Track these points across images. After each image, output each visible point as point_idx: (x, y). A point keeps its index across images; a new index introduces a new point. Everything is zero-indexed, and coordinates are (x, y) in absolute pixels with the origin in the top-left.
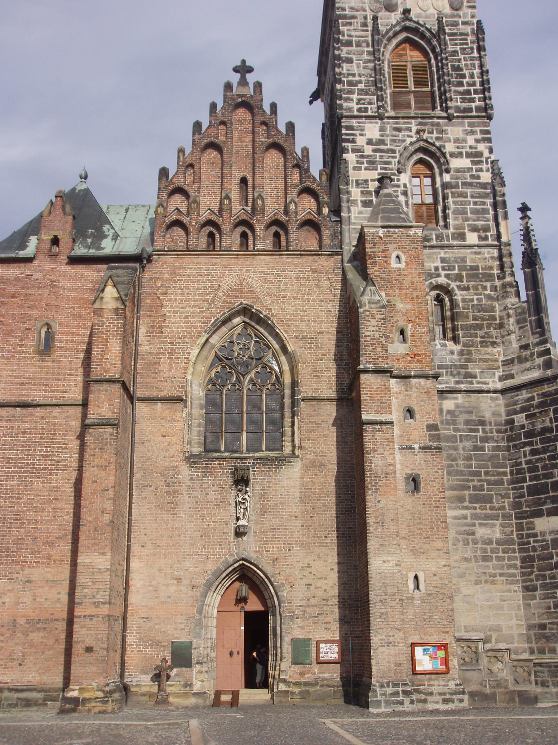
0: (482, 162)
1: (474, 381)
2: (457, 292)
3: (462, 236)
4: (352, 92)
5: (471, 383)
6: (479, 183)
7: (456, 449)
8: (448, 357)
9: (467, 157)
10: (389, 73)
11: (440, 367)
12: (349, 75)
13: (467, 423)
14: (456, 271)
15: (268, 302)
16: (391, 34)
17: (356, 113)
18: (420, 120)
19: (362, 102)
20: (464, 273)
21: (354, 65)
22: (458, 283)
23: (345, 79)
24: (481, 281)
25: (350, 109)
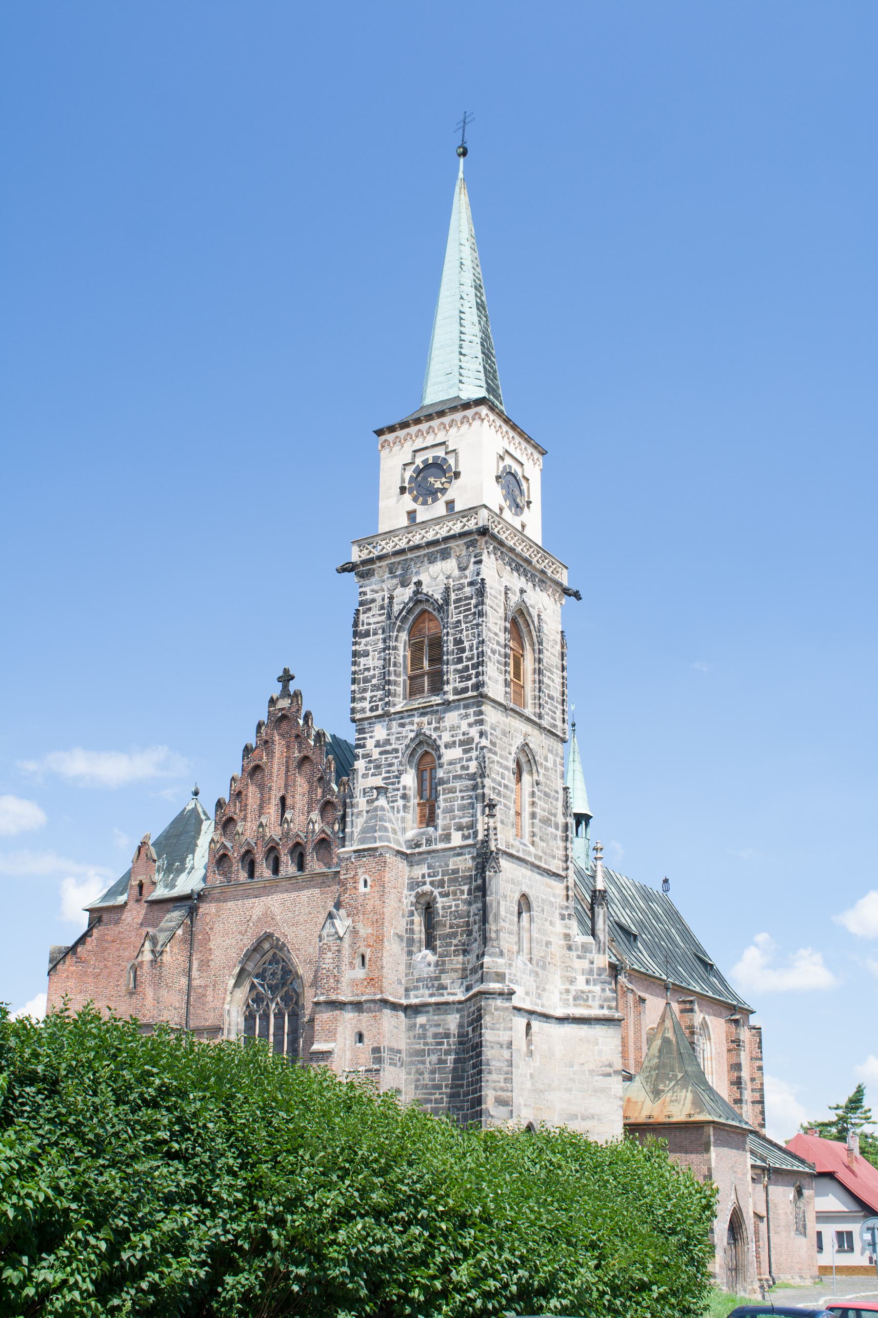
0: (472, 749)
1: (445, 992)
2: (439, 899)
3: (447, 838)
4: (365, 690)
5: (442, 995)
6: (467, 774)
7: (423, 1063)
8: (426, 969)
9: (459, 746)
10: (405, 656)
11: (418, 980)
12: (365, 670)
13: (435, 1036)
14: (440, 877)
15: (285, 929)
16: (404, 613)
17: (369, 714)
18: (421, 710)
19: (374, 699)
20: (446, 878)
21: (370, 657)
22: (440, 890)
23: (361, 676)
24: (460, 885)
25: (363, 710)
